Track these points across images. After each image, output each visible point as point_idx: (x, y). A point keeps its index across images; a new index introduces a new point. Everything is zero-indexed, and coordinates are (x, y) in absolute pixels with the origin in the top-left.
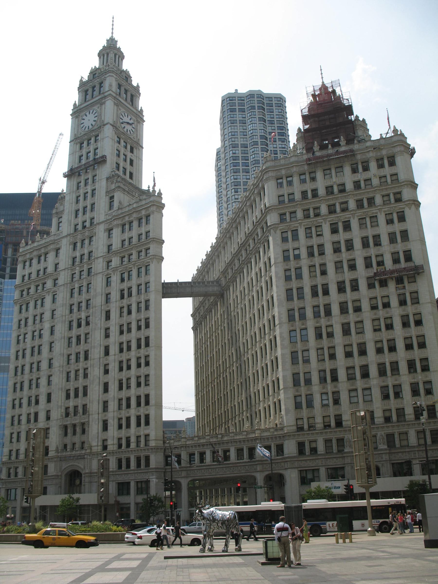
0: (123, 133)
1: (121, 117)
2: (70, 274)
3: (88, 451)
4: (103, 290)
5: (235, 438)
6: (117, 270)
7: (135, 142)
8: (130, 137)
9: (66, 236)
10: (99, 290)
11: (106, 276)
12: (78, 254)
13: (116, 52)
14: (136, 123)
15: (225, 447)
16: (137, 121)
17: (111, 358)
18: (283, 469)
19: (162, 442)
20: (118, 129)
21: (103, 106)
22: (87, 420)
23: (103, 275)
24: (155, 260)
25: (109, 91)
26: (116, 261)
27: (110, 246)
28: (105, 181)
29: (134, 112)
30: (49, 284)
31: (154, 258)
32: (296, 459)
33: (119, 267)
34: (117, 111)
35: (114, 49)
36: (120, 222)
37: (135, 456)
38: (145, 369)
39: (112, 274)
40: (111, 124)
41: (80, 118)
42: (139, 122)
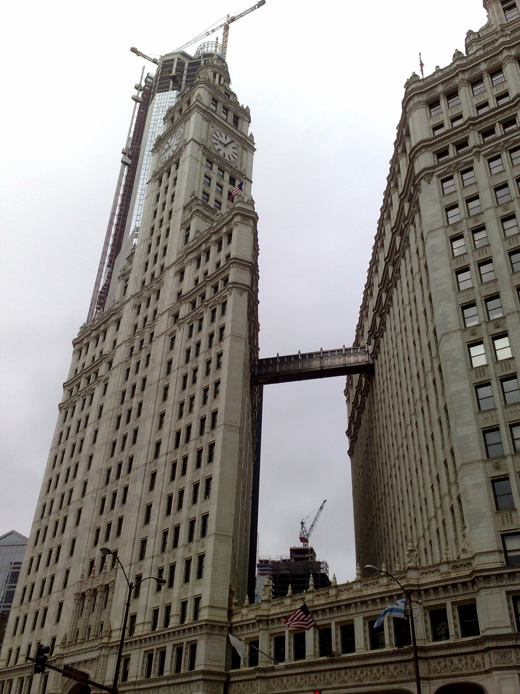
1: (214, 135)
2: (129, 349)
4: (164, 356)
5: (364, 593)
6: (183, 322)
7: (239, 172)
8: (230, 165)
9: (129, 300)
10: (159, 359)
11: (170, 335)
12: (141, 318)
13: (216, 70)
14: (240, 149)
15: (342, 616)
18: (481, 673)
19: (225, 613)
20: (208, 150)
21: (188, 123)
23: (166, 335)
24: (234, 288)
25: (195, 102)
26: (184, 310)
27: (180, 294)
28: (181, 210)
29: (238, 136)
30: (103, 369)
31: (232, 287)
32: (511, 643)
33: (187, 316)
34: (209, 128)
35: (213, 67)
36: (195, 254)
37: (174, 645)
38: (207, 469)
39: (178, 330)
40: (195, 141)
41: (161, 150)
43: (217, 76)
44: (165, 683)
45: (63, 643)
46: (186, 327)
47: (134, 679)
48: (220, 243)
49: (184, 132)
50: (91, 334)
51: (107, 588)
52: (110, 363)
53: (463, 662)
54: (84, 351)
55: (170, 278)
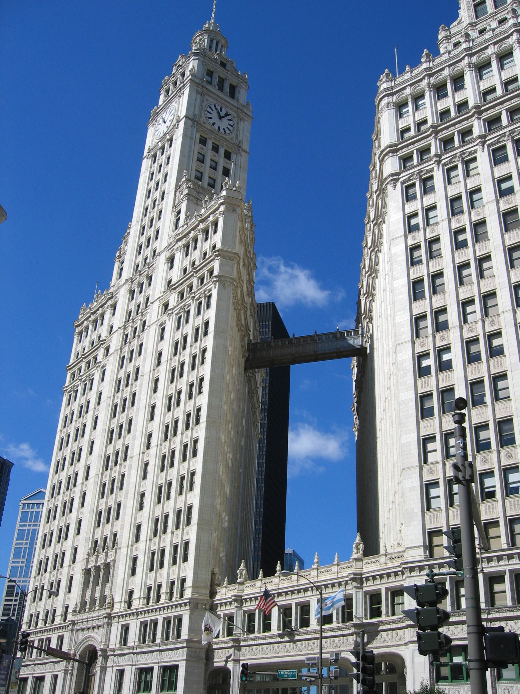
0: (210, 130)
3: (108, 611)
6: (172, 313)
7: (234, 144)
11: (161, 325)
14: (236, 120)
15: (301, 598)
16: (238, 117)
17: (153, 450)
18: (401, 645)
19: (207, 592)
22: (113, 558)
23: (157, 325)
26: (173, 299)
36: (184, 242)
39: (168, 320)
42: (242, 119)
43: (215, 42)
44: (157, 648)
45: (74, 611)
46: (174, 317)
47: (132, 644)
48: (206, 232)
49: (178, 107)
50: (89, 317)
51: (107, 566)
52: (108, 349)
53: (390, 636)
54: (84, 334)
55: (161, 263)
